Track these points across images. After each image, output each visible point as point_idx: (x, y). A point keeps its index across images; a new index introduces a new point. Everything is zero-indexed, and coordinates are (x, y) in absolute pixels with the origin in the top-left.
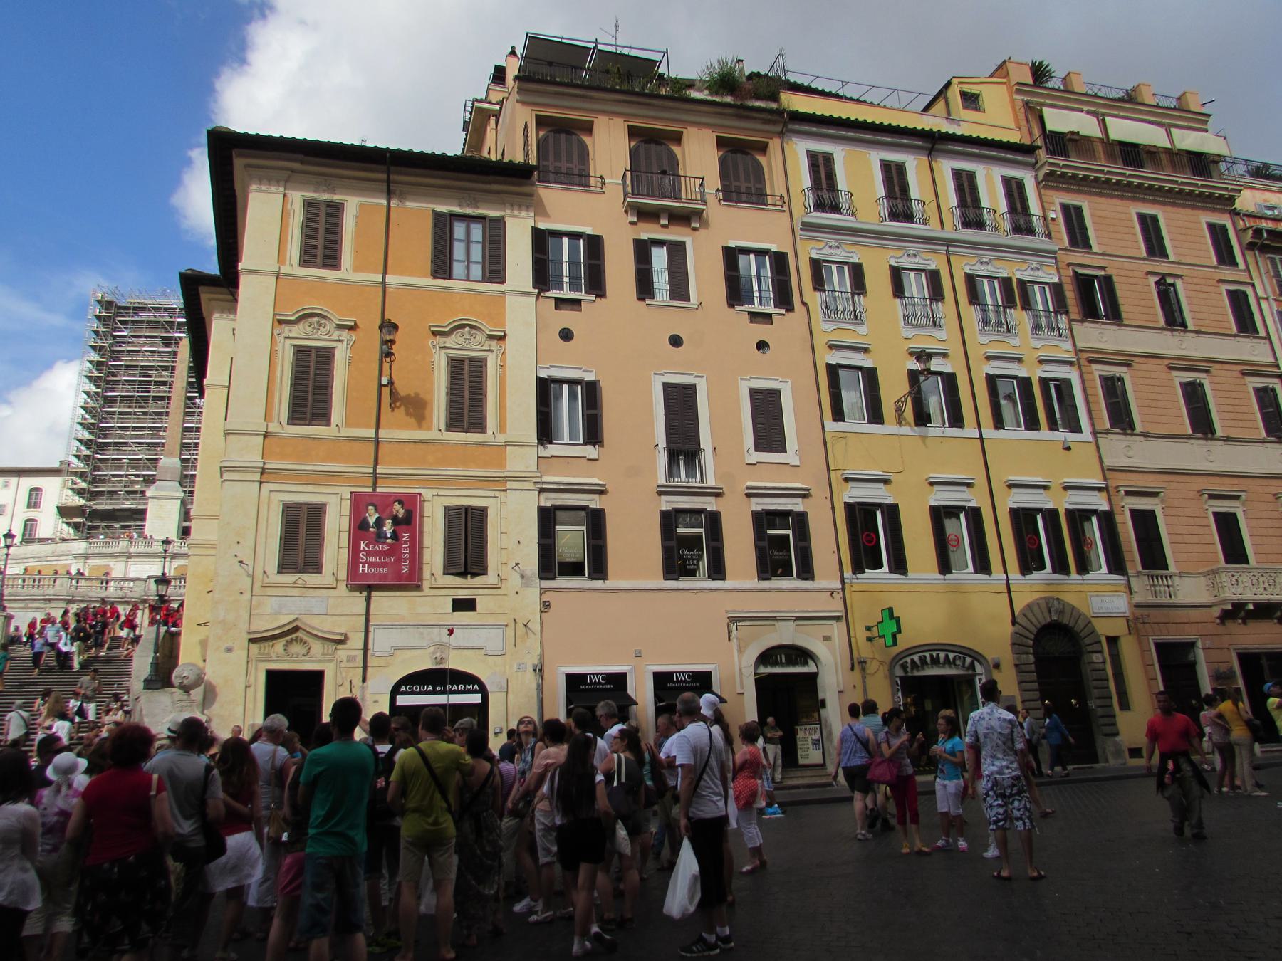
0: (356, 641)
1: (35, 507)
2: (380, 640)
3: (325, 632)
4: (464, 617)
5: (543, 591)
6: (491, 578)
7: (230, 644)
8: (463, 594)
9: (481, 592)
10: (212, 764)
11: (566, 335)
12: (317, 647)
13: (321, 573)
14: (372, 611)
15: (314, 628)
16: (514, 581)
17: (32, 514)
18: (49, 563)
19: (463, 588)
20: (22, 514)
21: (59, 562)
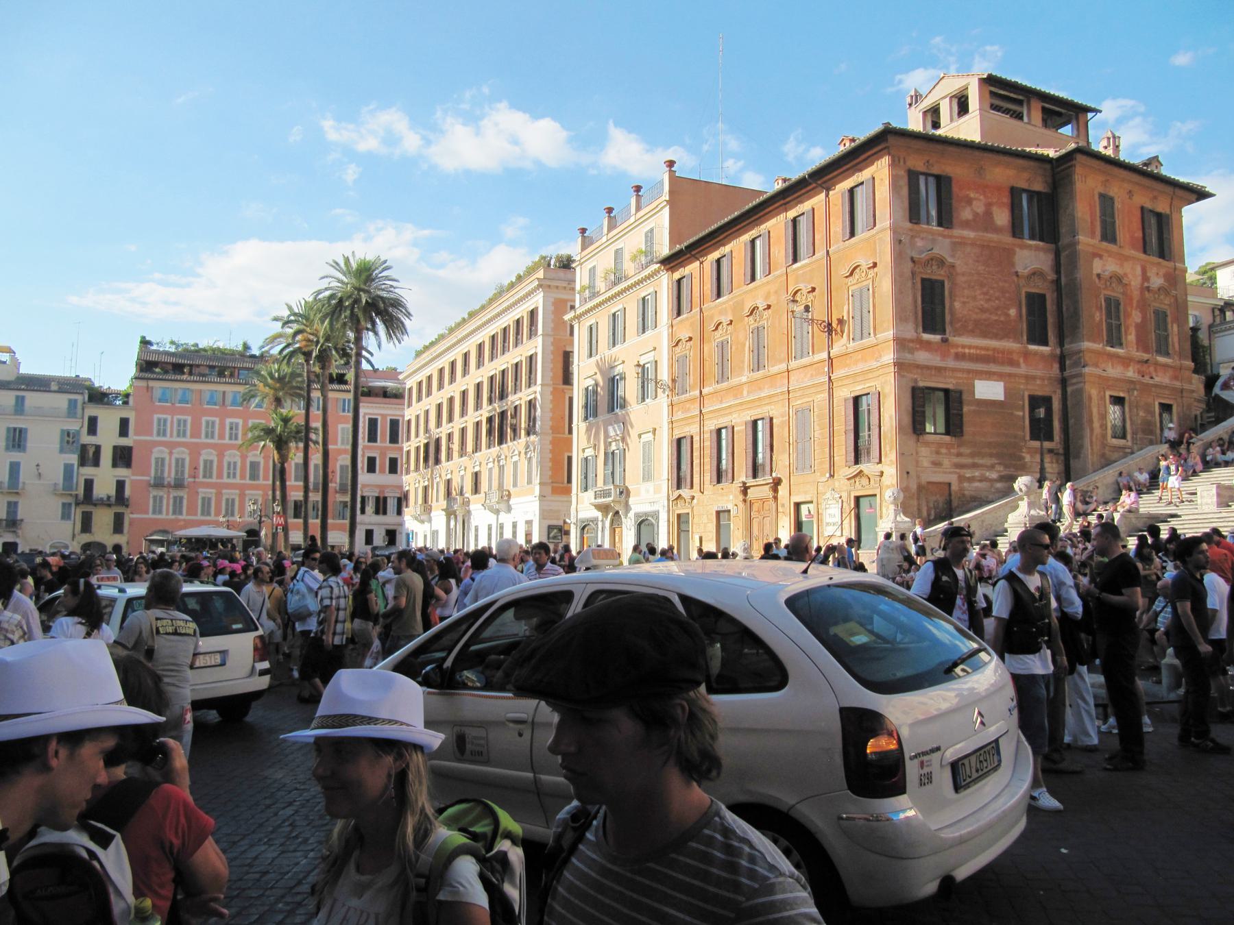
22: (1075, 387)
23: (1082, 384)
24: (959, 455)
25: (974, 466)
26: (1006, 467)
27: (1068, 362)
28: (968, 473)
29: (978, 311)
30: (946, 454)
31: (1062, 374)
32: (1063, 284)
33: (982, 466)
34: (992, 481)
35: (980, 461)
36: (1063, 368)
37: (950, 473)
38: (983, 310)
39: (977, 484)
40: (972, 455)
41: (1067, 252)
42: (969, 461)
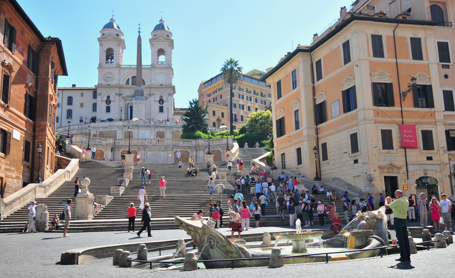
0: (404, 169)
1: (70, 104)
2: (411, 168)
3: (398, 166)
4: (430, 162)
5: (449, 154)
6: (435, 151)
7: (374, 169)
8: (429, 155)
9: (433, 155)
10: (315, 203)
11: (446, 76)
12: (395, 170)
13: (393, 149)
14: (407, 160)
15: (397, 166)
16: (441, 151)
17: (70, 107)
18: (108, 130)
19: (429, 153)
20: (66, 107)
21: (112, 130)
22: (40, 140)
23: (45, 140)
24: (6, 164)
25: (9, 170)
26: (17, 172)
27: (37, 129)
28: (9, 174)
29: (17, 97)
30: (3, 163)
31: (34, 133)
32: (38, 94)
33: (12, 171)
34: (13, 178)
35: (12, 168)
36: (34, 131)
37: (3, 172)
38: (18, 97)
39: (10, 179)
40: (10, 165)
41: (42, 81)
42: (9, 167)
